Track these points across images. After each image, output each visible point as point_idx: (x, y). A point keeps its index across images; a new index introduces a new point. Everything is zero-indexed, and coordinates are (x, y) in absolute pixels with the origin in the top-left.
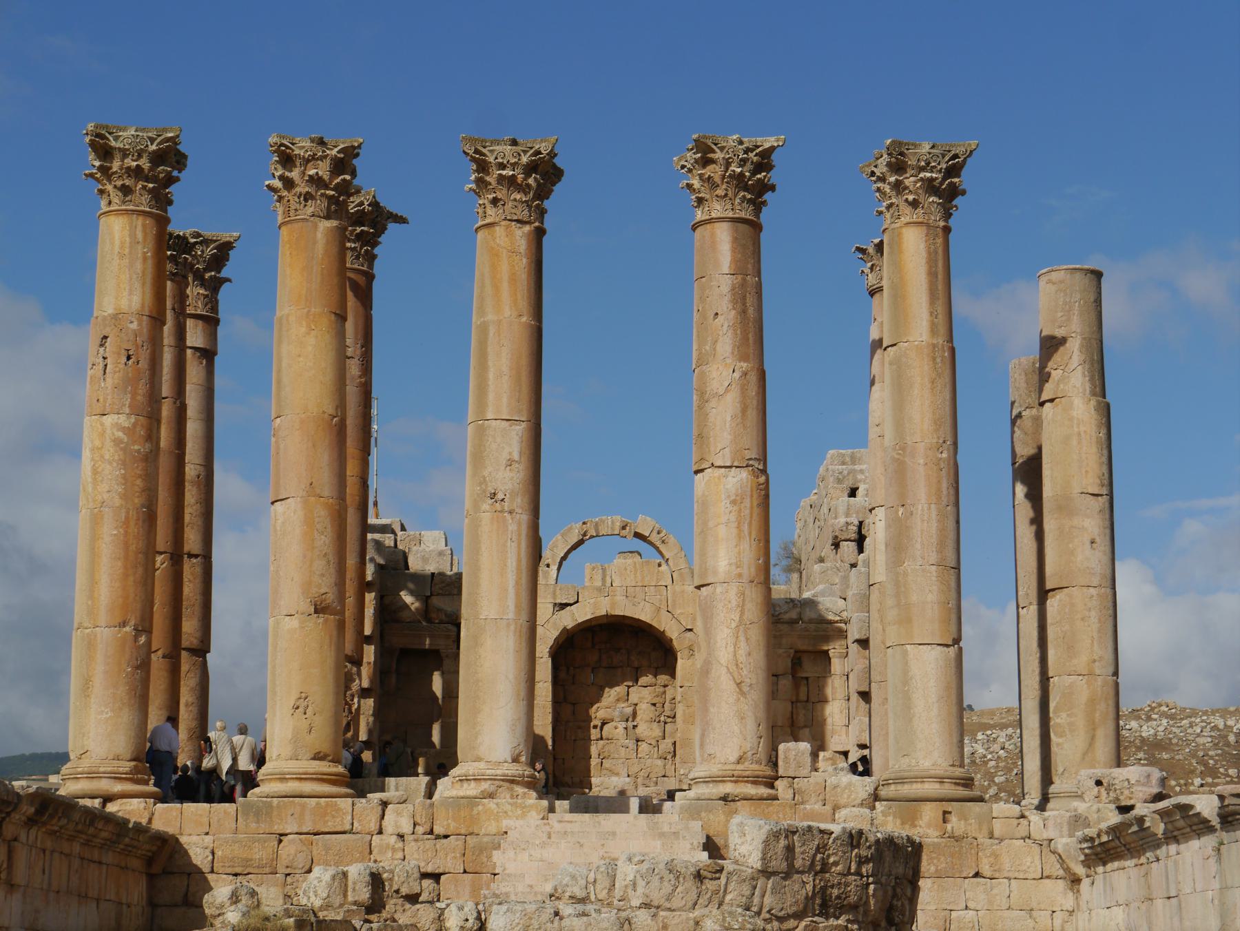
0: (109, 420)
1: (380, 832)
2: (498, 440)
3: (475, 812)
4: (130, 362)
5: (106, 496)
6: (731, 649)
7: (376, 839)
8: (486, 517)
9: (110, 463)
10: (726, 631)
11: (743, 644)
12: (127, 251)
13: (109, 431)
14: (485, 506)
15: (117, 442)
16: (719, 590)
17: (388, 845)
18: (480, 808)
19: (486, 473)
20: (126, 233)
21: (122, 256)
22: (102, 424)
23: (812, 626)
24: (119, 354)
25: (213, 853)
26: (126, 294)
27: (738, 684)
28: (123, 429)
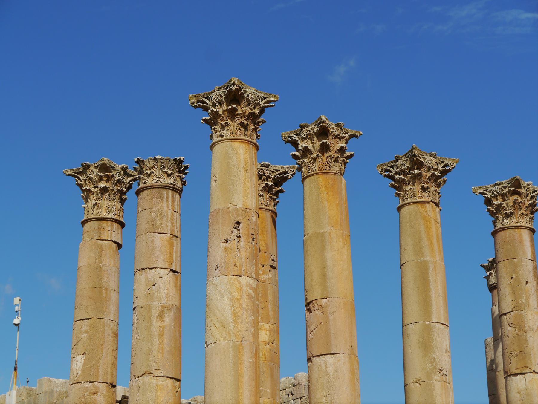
0: (244, 280)
2: (441, 336)
5: (245, 334)
8: (438, 385)
9: (247, 311)
12: (249, 168)
13: (244, 288)
19: (435, 356)
20: (248, 156)
21: (246, 171)
22: (240, 283)
24: (248, 236)
26: (250, 196)
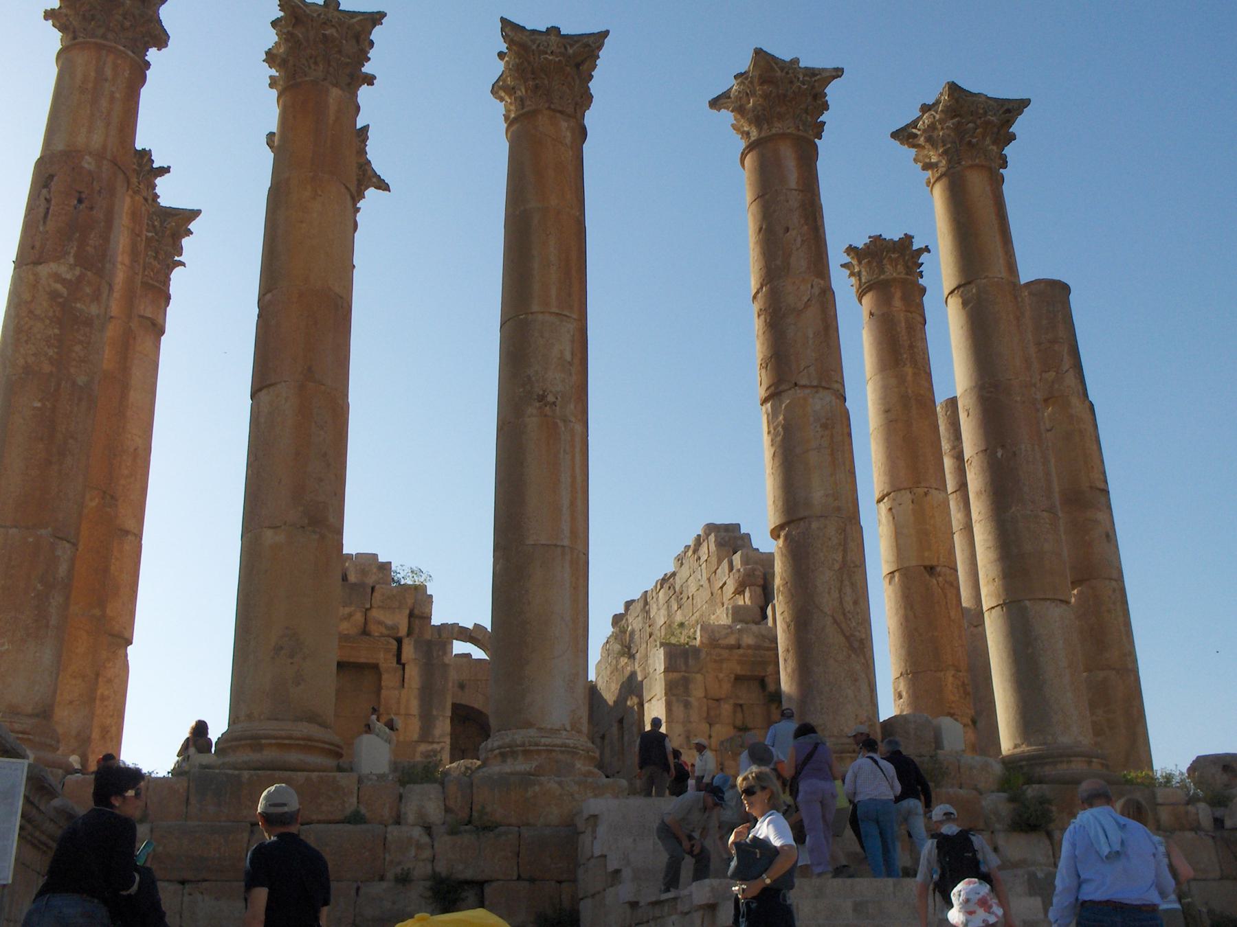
0: (44, 270)
1: (398, 821)
3: (530, 793)
4: (82, 207)
6: (836, 595)
7: (394, 832)
11: (848, 590)
12: (90, 85)
14: (530, 410)
15: (54, 295)
16: (814, 525)
18: (537, 788)
22: (35, 274)
23: (750, 651)
27: (847, 638)
28: (64, 281)
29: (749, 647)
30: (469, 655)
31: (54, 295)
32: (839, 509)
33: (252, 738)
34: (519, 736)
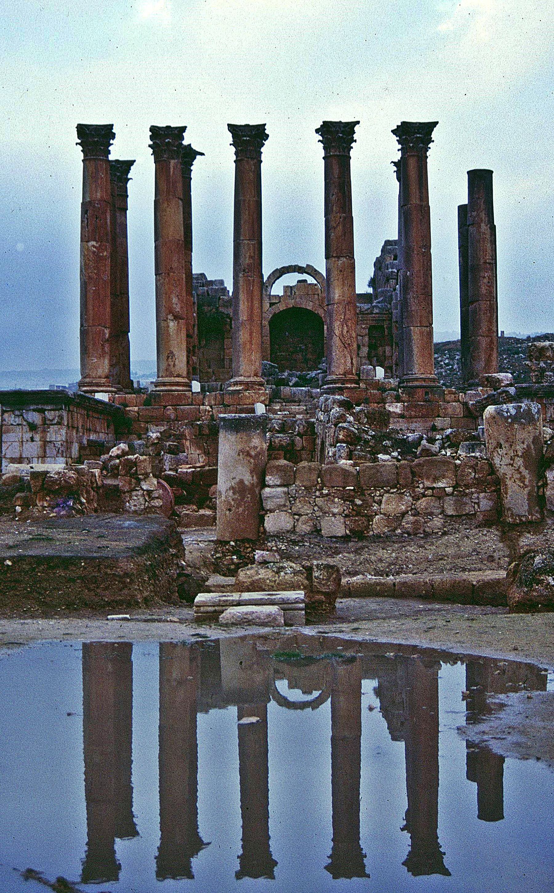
4: (98, 221)
7: (201, 407)
10: (339, 323)
11: (345, 328)
17: (206, 410)
25: (138, 414)
29: (376, 314)
30: (305, 281)
31: (94, 252)
32: (344, 300)
33: (163, 382)
34: (237, 379)
